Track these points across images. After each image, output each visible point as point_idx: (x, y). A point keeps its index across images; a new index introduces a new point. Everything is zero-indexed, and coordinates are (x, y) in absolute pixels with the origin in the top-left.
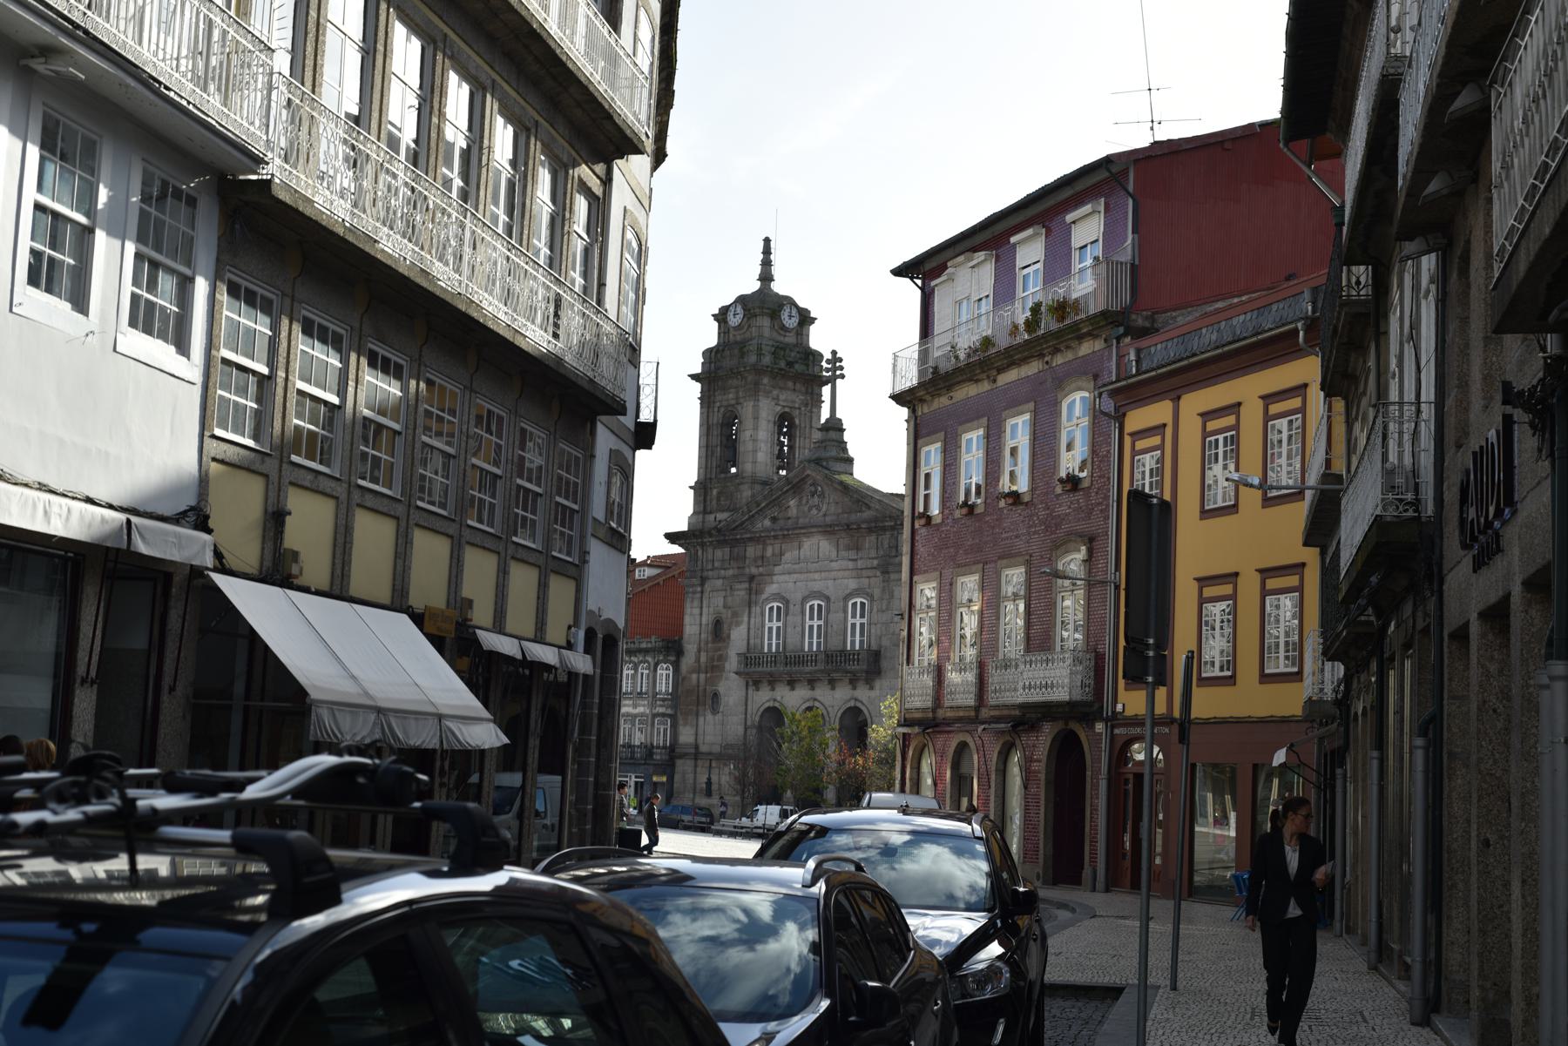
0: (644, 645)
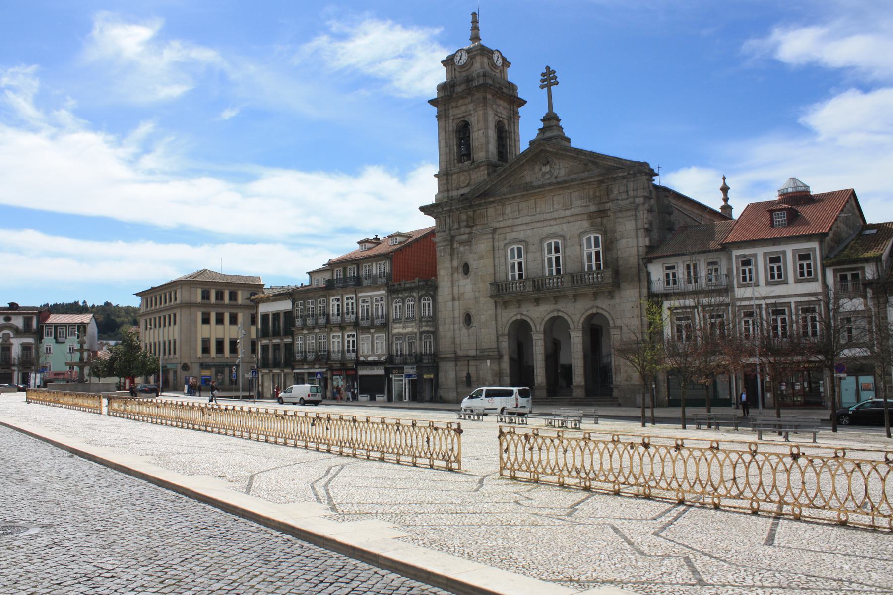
0: (407, 285)
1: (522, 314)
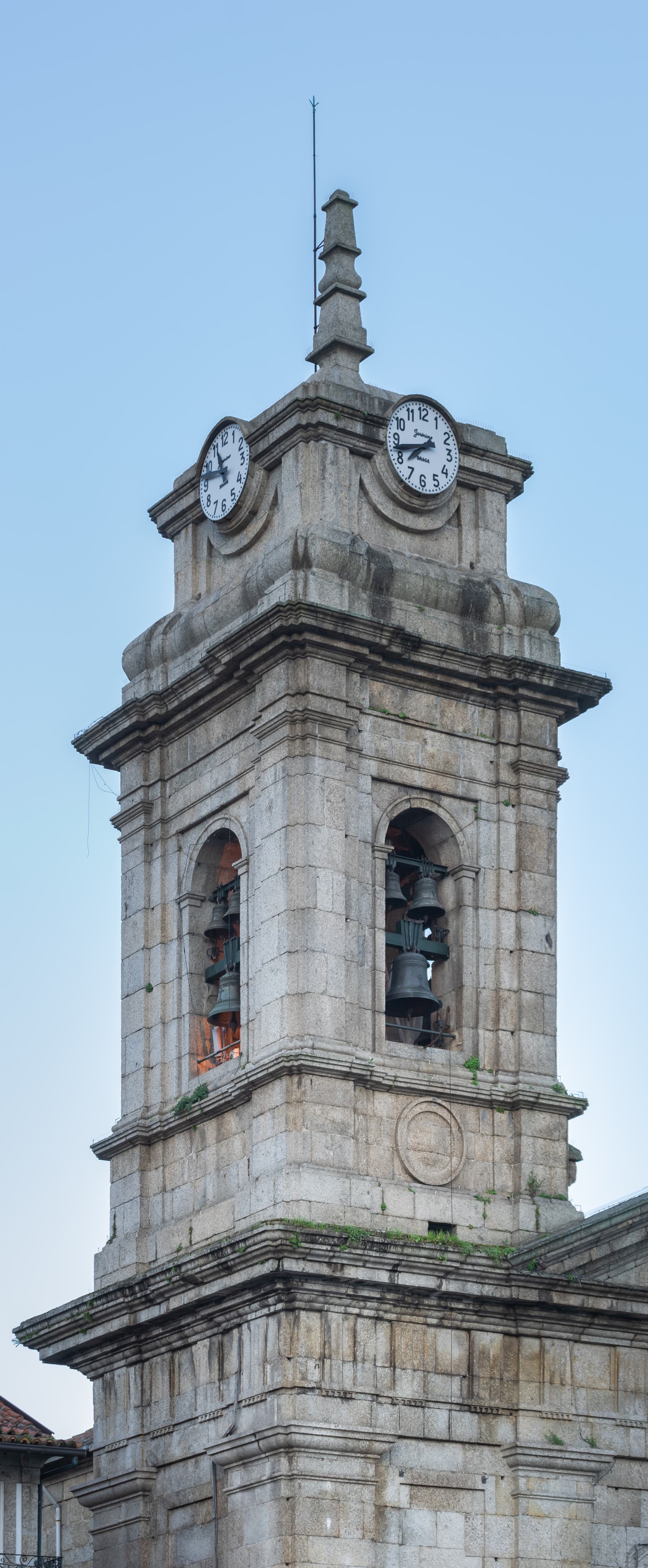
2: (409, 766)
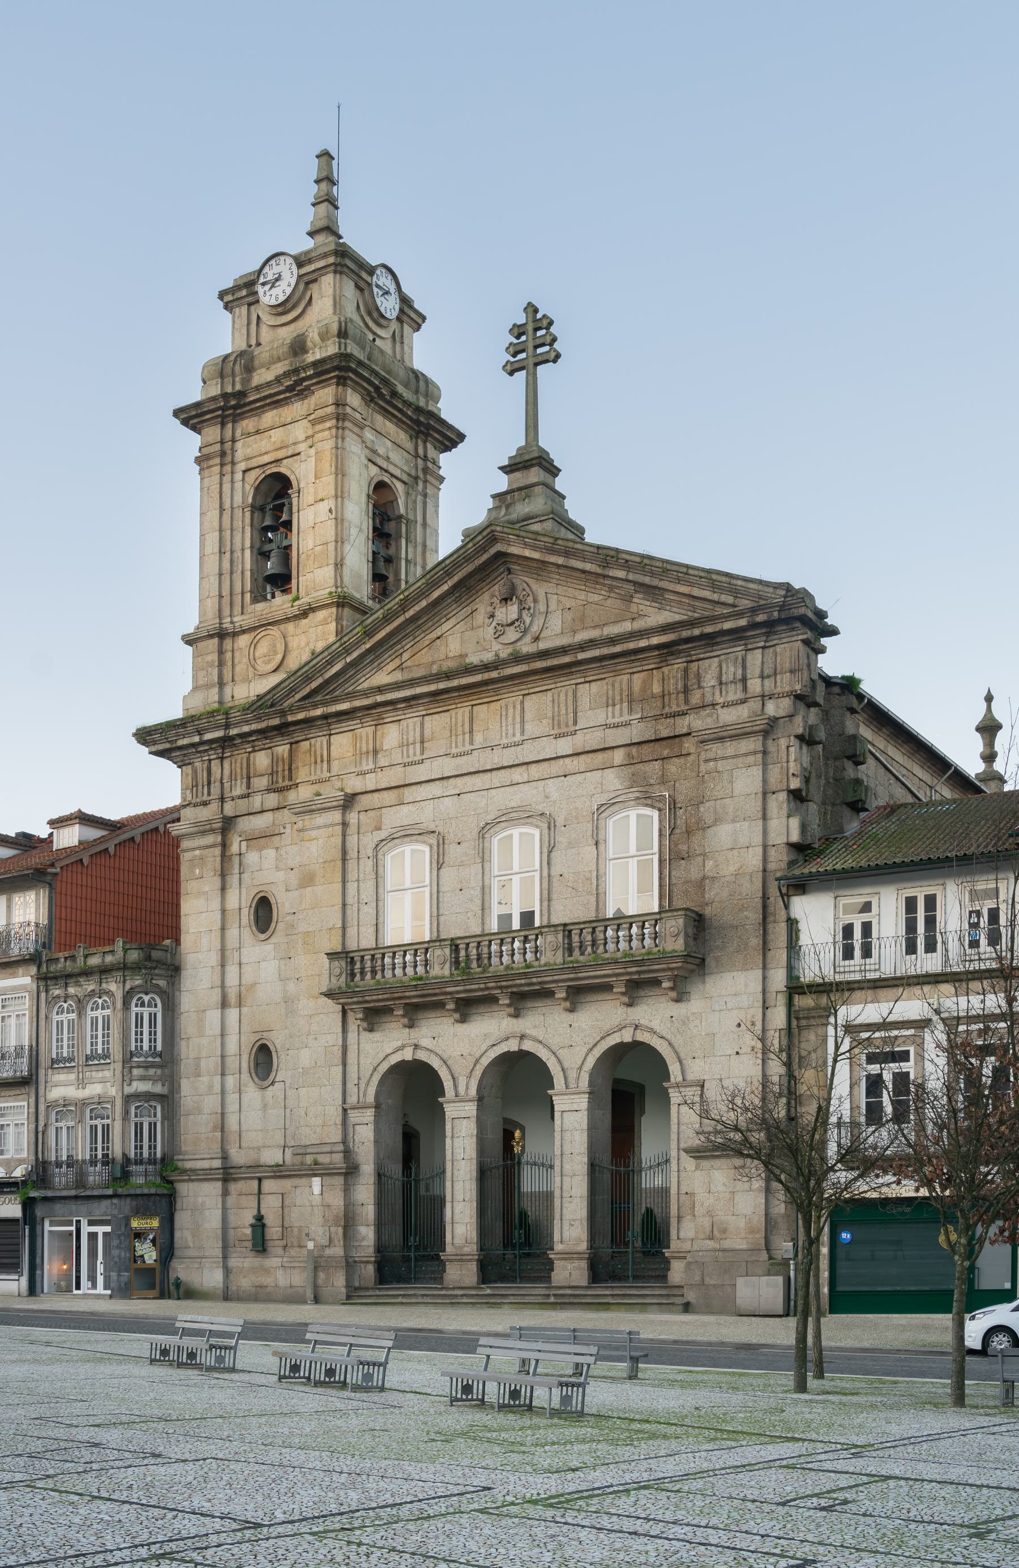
0: (94, 961)
1: (416, 1047)
2: (260, 455)
